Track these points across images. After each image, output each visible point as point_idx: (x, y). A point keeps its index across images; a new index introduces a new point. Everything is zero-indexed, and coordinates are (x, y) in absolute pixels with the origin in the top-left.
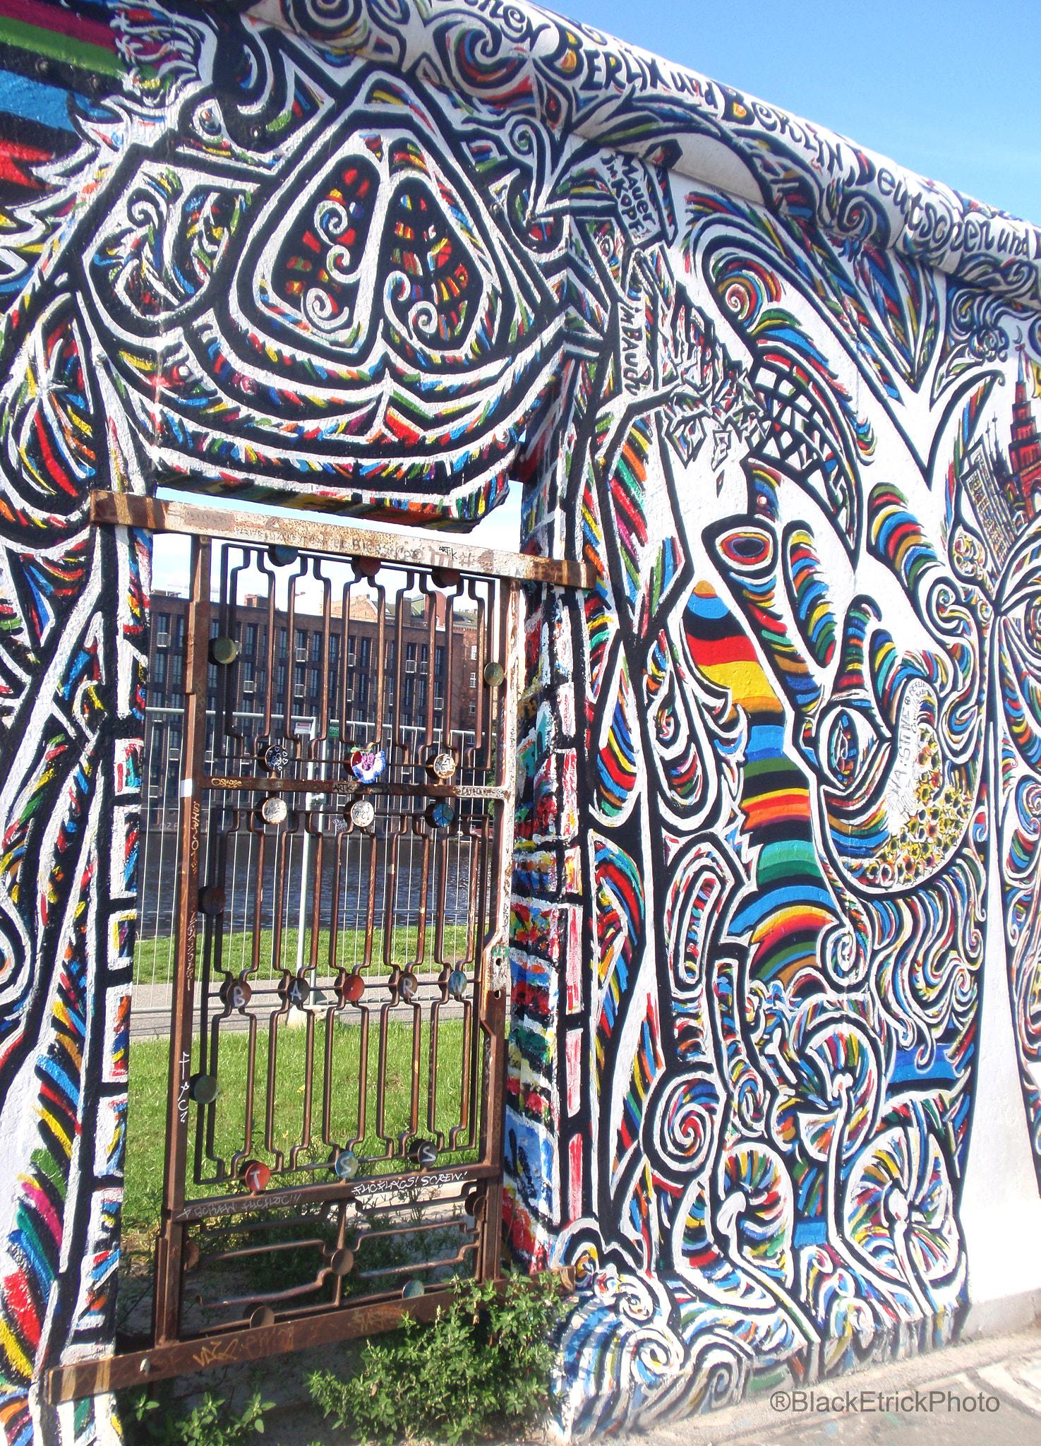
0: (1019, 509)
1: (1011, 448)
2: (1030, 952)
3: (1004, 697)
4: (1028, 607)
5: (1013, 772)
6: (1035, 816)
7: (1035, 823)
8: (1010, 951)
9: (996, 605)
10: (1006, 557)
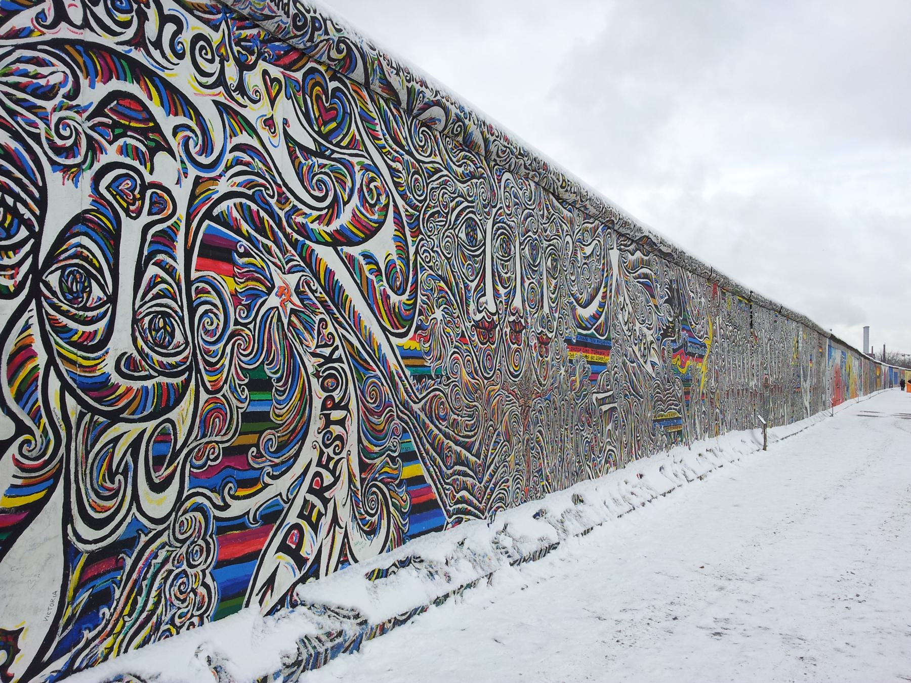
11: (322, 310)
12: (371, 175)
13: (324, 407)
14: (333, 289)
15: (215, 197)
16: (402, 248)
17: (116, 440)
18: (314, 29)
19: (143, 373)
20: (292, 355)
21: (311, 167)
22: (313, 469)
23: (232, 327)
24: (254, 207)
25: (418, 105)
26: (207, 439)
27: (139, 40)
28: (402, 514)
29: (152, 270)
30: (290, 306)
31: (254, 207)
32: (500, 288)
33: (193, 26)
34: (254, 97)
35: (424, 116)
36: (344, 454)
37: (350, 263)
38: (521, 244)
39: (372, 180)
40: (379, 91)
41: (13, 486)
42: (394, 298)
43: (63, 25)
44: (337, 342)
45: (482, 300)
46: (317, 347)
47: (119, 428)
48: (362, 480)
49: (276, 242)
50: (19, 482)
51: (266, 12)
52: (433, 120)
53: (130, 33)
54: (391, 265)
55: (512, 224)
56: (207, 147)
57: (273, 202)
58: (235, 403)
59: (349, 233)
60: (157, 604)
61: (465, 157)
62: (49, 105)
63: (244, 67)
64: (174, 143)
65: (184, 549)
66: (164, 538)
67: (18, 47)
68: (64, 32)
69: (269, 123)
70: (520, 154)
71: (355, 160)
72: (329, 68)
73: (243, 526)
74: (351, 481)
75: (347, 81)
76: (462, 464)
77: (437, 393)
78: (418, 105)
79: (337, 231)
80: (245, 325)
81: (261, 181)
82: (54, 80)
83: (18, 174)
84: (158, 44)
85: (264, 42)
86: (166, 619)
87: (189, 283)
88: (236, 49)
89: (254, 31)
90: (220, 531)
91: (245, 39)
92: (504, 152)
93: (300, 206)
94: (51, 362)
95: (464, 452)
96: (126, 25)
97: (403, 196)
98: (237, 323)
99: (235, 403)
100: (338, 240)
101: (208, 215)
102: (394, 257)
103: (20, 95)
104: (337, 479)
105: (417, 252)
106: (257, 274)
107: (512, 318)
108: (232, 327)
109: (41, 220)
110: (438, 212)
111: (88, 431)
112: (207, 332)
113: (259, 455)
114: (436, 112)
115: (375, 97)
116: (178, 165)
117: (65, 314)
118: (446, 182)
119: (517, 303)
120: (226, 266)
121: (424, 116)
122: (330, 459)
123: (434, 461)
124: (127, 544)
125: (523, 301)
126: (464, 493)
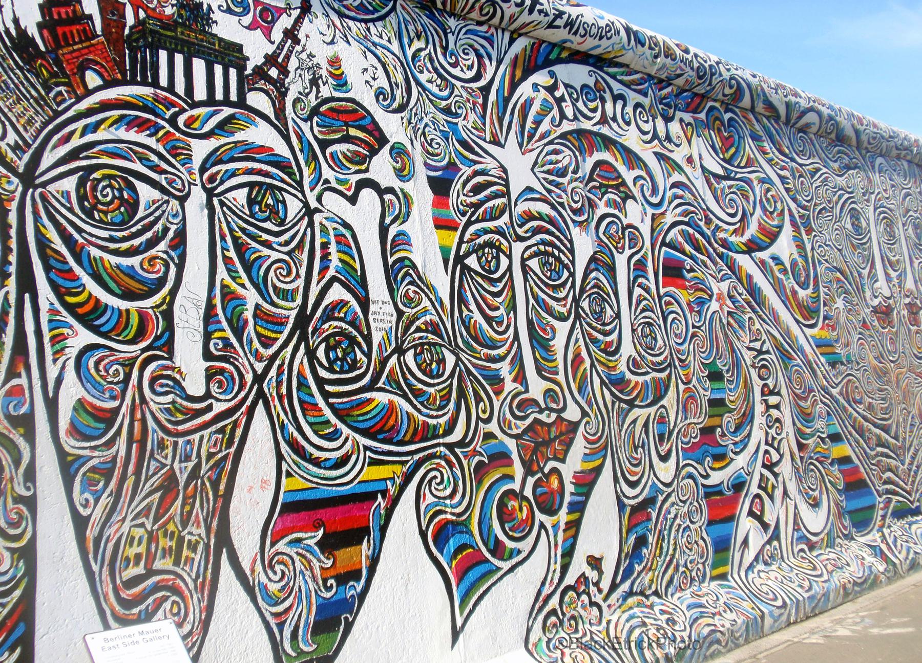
0: (57, 85)
1: (40, 26)
2: (116, 517)
3: (48, 268)
4: (81, 183)
5: (69, 342)
6: (111, 383)
7: (112, 390)
8: (80, 523)
9: (28, 178)
10: (39, 132)
11: (749, 310)
12: (767, 186)
13: (763, 394)
14: (753, 290)
15: (666, 228)
16: (801, 246)
17: (634, 422)
18: (712, 74)
19: (643, 370)
20: (733, 351)
21: (723, 190)
22: (763, 447)
23: (691, 331)
24: (691, 231)
25: (795, 115)
26: (688, 421)
27: (603, 121)
28: (838, 490)
29: (638, 291)
30: (726, 309)
31: (691, 231)
32: (890, 271)
33: (633, 97)
34: (677, 142)
35: (798, 125)
36: (784, 435)
37: (762, 265)
38: (904, 225)
39: (768, 190)
40: (762, 111)
41: (585, 454)
42: (802, 294)
43: (565, 121)
44: (764, 337)
45: (877, 285)
46: (751, 341)
47: (636, 412)
48: (801, 458)
49: (709, 257)
50: (588, 451)
51: (679, 72)
52: (808, 125)
53: (598, 115)
54: (794, 264)
55: (892, 206)
56: (654, 191)
57: (702, 224)
58: (702, 391)
59: (758, 241)
60: (675, 550)
61: (839, 152)
62: (564, 180)
63: (668, 119)
64: (635, 191)
65: (686, 509)
66: (672, 499)
67: (545, 145)
68: (567, 126)
69: (690, 160)
70: (890, 137)
71: (753, 176)
72: (722, 102)
73: (720, 493)
74: (793, 459)
75: (737, 110)
76: (883, 446)
77: (851, 377)
78: (795, 115)
79: (749, 240)
80: (699, 328)
81: (692, 209)
82: (565, 162)
83: (558, 234)
84: (614, 119)
85: (677, 95)
86: (682, 562)
87: (660, 298)
88: (660, 107)
89: (669, 89)
90: (707, 495)
91: (665, 98)
92: (874, 138)
93: (721, 224)
94: (592, 365)
95: (883, 434)
96: (594, 110)
97: (794, 200)
98: (694, 327)
99: (702, 391)
100: (752, 247)
101: (663, 244)
102: (796, 256)
103: (551, 178)
104: (782, 456)
105: (813, 249)
106: (700, 286)
107: (907, 301)
108: (691, 331)
109: (573, 262)
110: (824, 208)
111: (618, 414)
112: (676, 335)
113: (723, 435)
114: (811, 117)
115: (759, 117)
116: (640, 208)
117: (594, 328)
118: (826, 179)
119: (910, 284)
120: (680, 282)
121: (798, 125)
122: (774, 439)
123: (857, 442)
124: (650, 501)
125: (916, 282)
126: (889, 474)
